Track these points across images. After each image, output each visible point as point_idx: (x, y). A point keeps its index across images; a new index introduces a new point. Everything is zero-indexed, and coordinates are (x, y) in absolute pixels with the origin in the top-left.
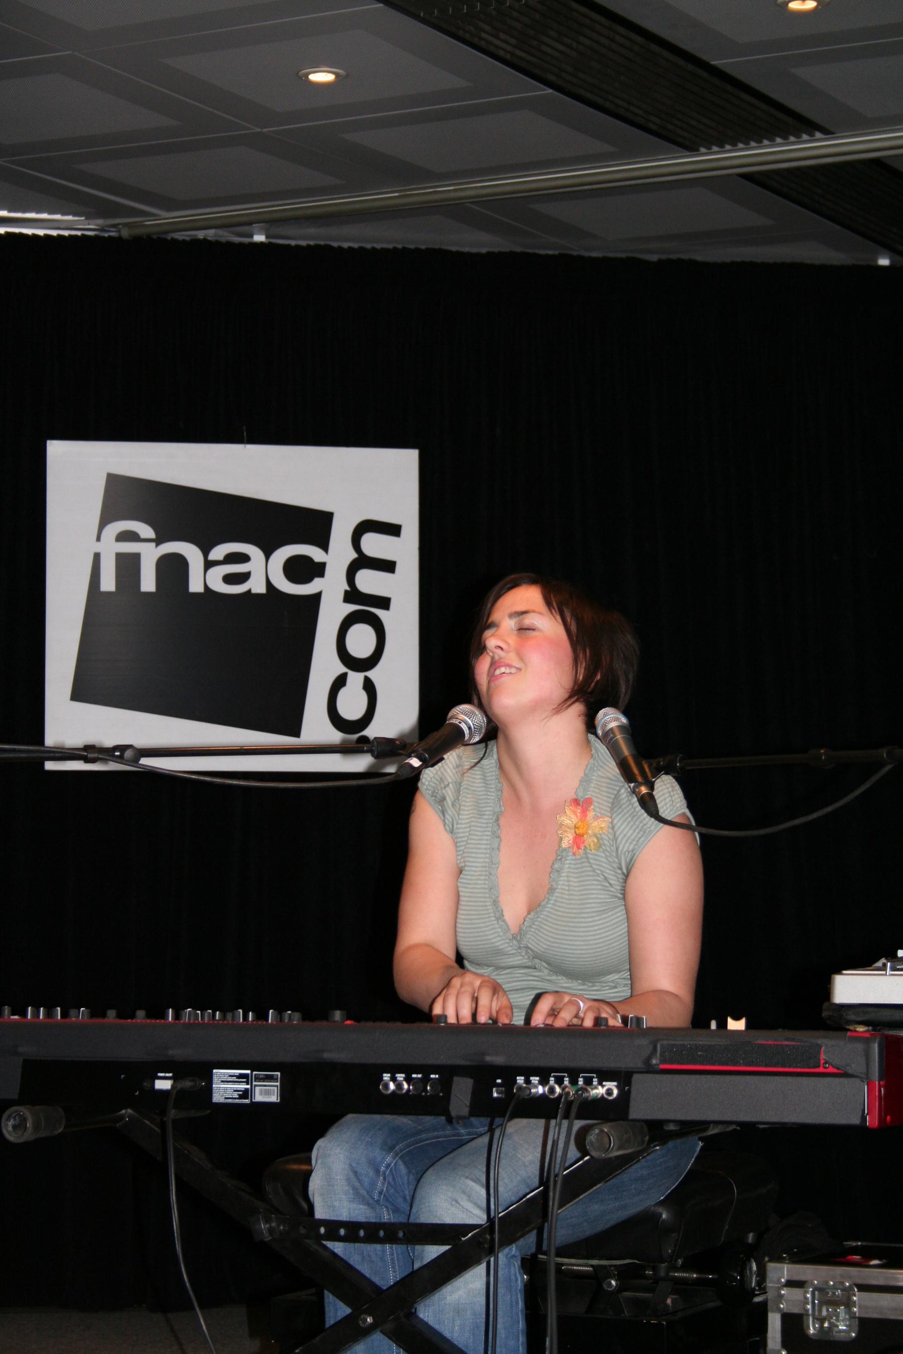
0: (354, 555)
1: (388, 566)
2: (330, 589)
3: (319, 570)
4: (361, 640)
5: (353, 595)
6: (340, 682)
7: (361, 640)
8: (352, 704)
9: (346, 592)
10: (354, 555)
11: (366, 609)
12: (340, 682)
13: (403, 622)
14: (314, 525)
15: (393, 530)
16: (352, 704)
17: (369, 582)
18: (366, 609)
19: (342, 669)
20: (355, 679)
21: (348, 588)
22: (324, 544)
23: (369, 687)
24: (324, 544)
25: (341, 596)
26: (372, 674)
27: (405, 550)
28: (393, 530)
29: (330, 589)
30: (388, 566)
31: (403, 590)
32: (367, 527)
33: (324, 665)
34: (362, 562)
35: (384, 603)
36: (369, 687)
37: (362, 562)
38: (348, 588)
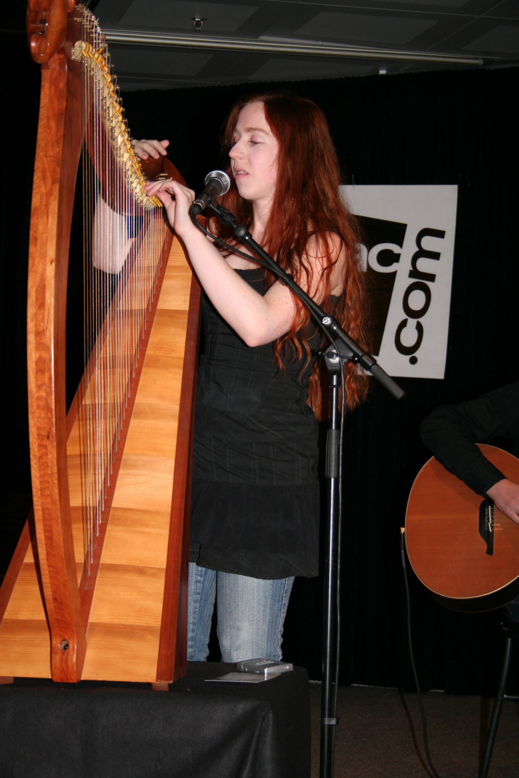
0: (416, 249)
1: (436, 256)
2: (402, 269)
3: (395, 258)
4: (417, 300)
5: (414, 273)
6: (403, 324)
7: (417, 300)
8: (409, 338)
9: (411, 271)
10: (416, 249)
11: (421, 281)
12: (403, 324)
13: (442, 290)
14: (395, 232)
15: (440, 234)
16: (409, 338)
17: (425, 265)
18: (421, 281)
19: (405, 317)
20: (412, 323)
21: (412, 269)
22: (401, 245)
23: (419, 328)
24: (401, 245)
25: (407, 273)
26: (421, 320)
27: (446, 247)
28: (440, 234)
29: (402, 269)
30: (436, 256)
31: (443, 270)
32: (426, 232)
33: (395, 314)
34: (422, 253)
35: (432, 277)
36: (419, 328)
37: (422, 253)
38: (412, 269)
